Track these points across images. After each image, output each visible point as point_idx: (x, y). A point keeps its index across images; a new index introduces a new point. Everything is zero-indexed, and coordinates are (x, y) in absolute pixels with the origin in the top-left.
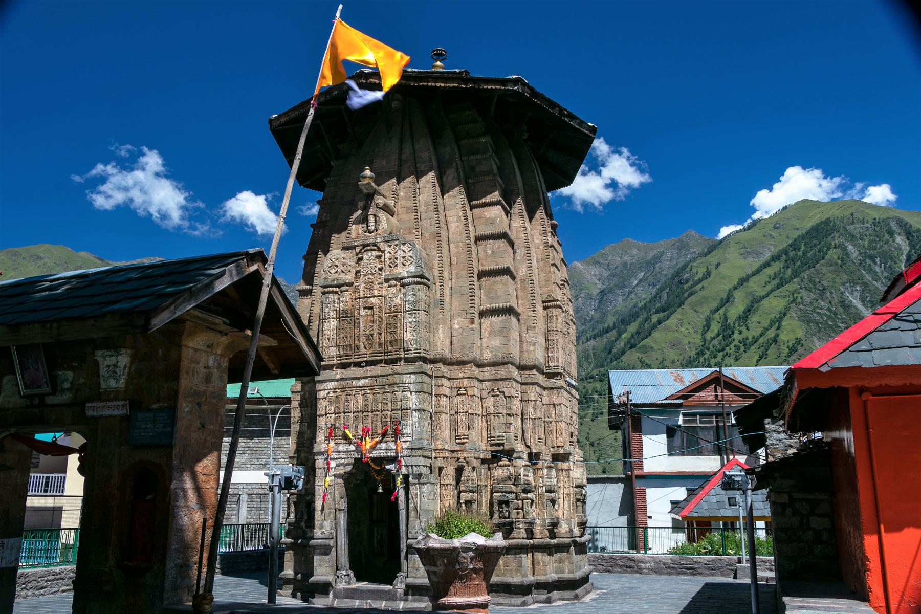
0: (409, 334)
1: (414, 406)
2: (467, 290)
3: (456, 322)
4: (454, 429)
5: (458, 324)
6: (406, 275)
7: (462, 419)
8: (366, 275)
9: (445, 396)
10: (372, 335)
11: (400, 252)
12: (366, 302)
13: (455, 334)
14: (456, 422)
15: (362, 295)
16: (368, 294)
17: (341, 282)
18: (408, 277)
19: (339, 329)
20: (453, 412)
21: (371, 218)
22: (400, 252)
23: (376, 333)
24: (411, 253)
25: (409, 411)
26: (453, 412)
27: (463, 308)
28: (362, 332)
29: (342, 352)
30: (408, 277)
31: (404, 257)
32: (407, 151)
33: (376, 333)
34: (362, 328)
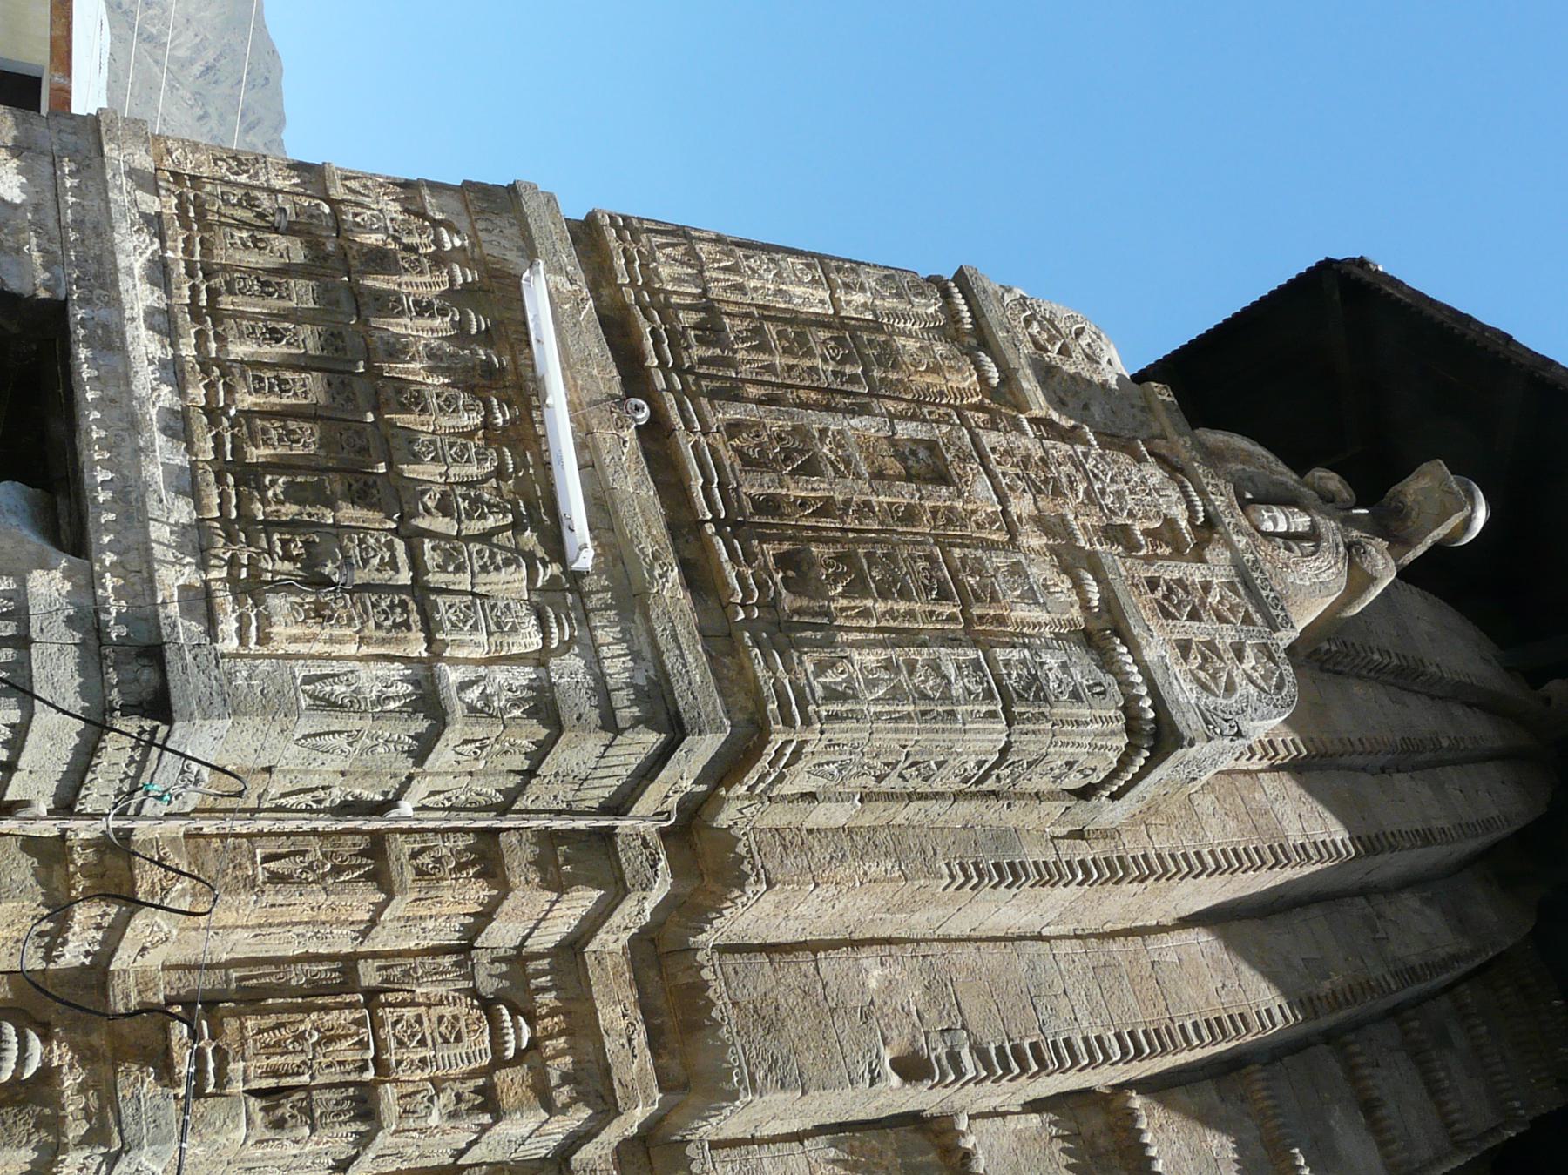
0: (871, 658)
1: (453, 676)
2: (1058, 1029)
3: (894, 971)
4: (252, 992)
5: (889, 986)
6: (1150, 655)
7: (330, 1048)
8: (1079, 466)
9: (485, 916)
10: (811, 468)
11: (1227, 636)
12: (964, 459)
13: (831, 964)
14: (312, 995)
15: (990, 439)
16: (1007, 471)
17: (1010, 354)
18: (1144, 669)
19: (797, 325)
20: (369, 975)
21: (1301, 522)
22: (1227, 636)
23: (816, 488)
24: (1244, 688)
25: (419, 649)
26: (369, 975)
27: (974, 1019)
28: (815, 421)
29: (687, 319)
30: (1144, 669)
31: (1210, 645)
32: (1480, 730)
33: (816, 488)
34: (834, 423)
